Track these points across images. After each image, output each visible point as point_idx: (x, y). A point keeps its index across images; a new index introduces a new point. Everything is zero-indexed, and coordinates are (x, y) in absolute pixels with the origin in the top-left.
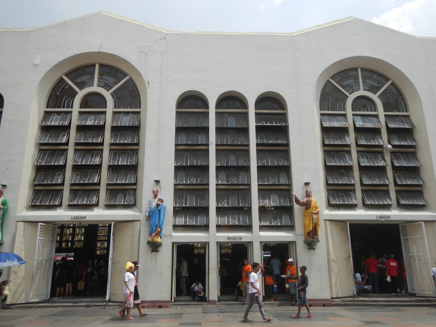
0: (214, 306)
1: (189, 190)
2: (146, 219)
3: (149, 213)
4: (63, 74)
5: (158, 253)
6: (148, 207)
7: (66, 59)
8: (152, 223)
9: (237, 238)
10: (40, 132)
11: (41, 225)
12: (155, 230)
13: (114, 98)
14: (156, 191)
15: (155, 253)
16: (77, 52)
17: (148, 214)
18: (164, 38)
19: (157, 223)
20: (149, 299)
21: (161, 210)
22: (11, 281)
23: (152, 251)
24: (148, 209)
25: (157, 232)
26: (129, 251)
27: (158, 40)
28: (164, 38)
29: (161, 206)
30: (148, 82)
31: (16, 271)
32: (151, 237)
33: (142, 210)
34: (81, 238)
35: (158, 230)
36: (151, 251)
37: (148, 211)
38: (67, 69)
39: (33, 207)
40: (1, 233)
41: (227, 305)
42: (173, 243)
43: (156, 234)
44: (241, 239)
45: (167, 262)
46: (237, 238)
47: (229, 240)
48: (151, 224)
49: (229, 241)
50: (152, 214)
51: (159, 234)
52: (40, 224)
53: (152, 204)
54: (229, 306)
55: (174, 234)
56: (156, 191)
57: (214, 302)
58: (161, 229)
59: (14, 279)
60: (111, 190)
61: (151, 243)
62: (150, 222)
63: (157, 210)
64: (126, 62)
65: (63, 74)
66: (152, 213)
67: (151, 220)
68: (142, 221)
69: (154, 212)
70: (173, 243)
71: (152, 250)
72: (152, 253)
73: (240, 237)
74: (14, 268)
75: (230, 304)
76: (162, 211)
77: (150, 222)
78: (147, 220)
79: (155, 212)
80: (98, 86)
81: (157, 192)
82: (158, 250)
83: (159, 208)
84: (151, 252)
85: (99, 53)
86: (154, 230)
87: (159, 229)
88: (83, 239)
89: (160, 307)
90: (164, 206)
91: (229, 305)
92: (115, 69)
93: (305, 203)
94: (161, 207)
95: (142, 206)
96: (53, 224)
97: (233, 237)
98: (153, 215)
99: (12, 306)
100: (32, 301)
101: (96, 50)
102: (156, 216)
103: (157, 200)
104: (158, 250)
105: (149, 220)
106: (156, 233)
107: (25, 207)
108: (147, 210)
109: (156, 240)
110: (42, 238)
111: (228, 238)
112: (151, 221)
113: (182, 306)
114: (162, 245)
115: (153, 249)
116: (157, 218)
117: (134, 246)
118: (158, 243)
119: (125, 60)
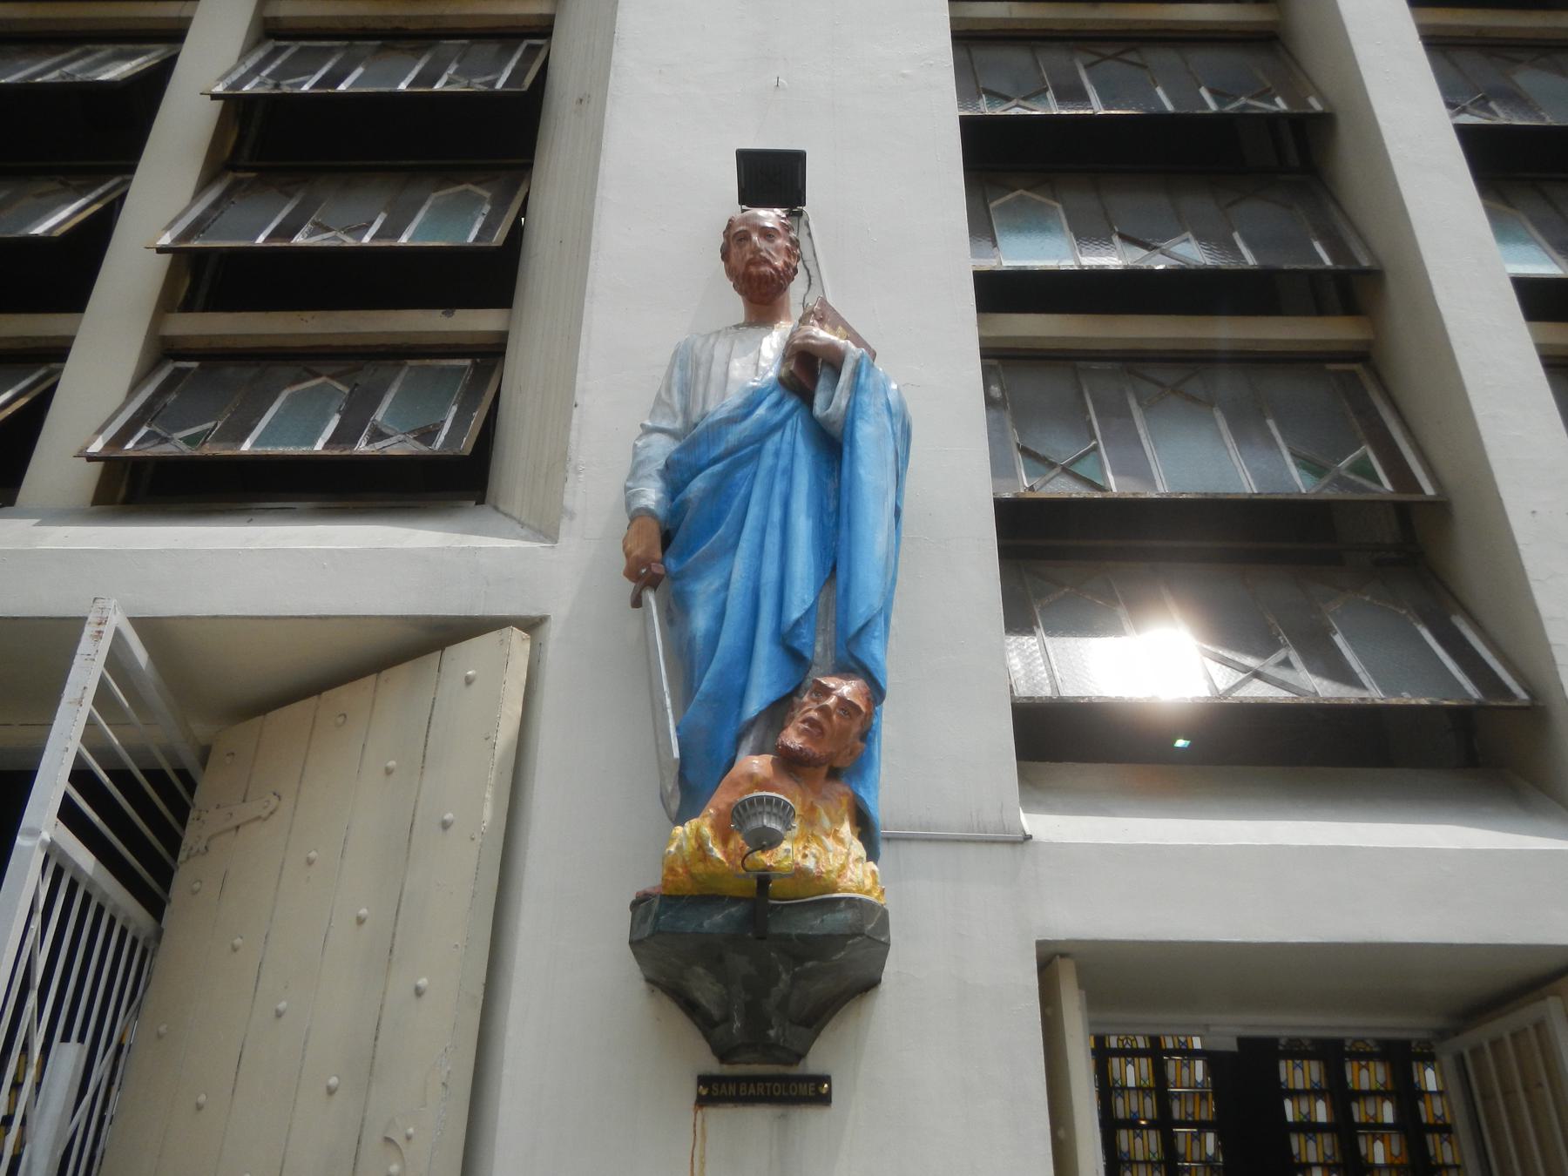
1: (1133, 361)
2: (632, 573)
3: (676, 476)
5: (810, 1119)
6: (648, 431)
8: (720, 616)
12: (779, 711)
15: (758, 1120)
17: (651, 495)
19: (801, 596)
24: (661, 448)
25: (815, 729)
26: (331, 1091)
29: (856, 373)
32: (722, 799)
33: (568, 501)
35: (827, 692)
36: (690, 1091)
37: (662, 461)
42: (1050, 960)
43: (791, 763)
48: (701, 621)
50: (720, 491)
51: (834, 774)
53: (717, 370)
55: (1043, 825)
58: (876, 692)
60: (216, 356)
61: (714, 921)
62: (677, 611)
63: (796, 426)
66: (725, 476)
67: (697, 574)
68: (553, 633)
69: (748, 453)
70: (1050, 960)
71: (713, 1066)
72: (720, 1117)
76: (870, 438)
77: (677, 611)
78: (643, 576)
79: (767, 460)
82: (814, 1063)
83: (830, 402)
84: (702, 1101)
86: (754, 706)
87: (847, 688)
94: (855, 388)
95: (563, 457)
98: (736, 502)
102: (776, 513)
103: (772, 344)
104: (814, 1063)
105: (678, 577)
106: (793, 738)
108: (635, 455)
109: (789, 854)
112: (703, 591)
114: (870, 984)
115: (723, 1055)
116: (803, 527)
117: (419, 992)
118: (844, 917)
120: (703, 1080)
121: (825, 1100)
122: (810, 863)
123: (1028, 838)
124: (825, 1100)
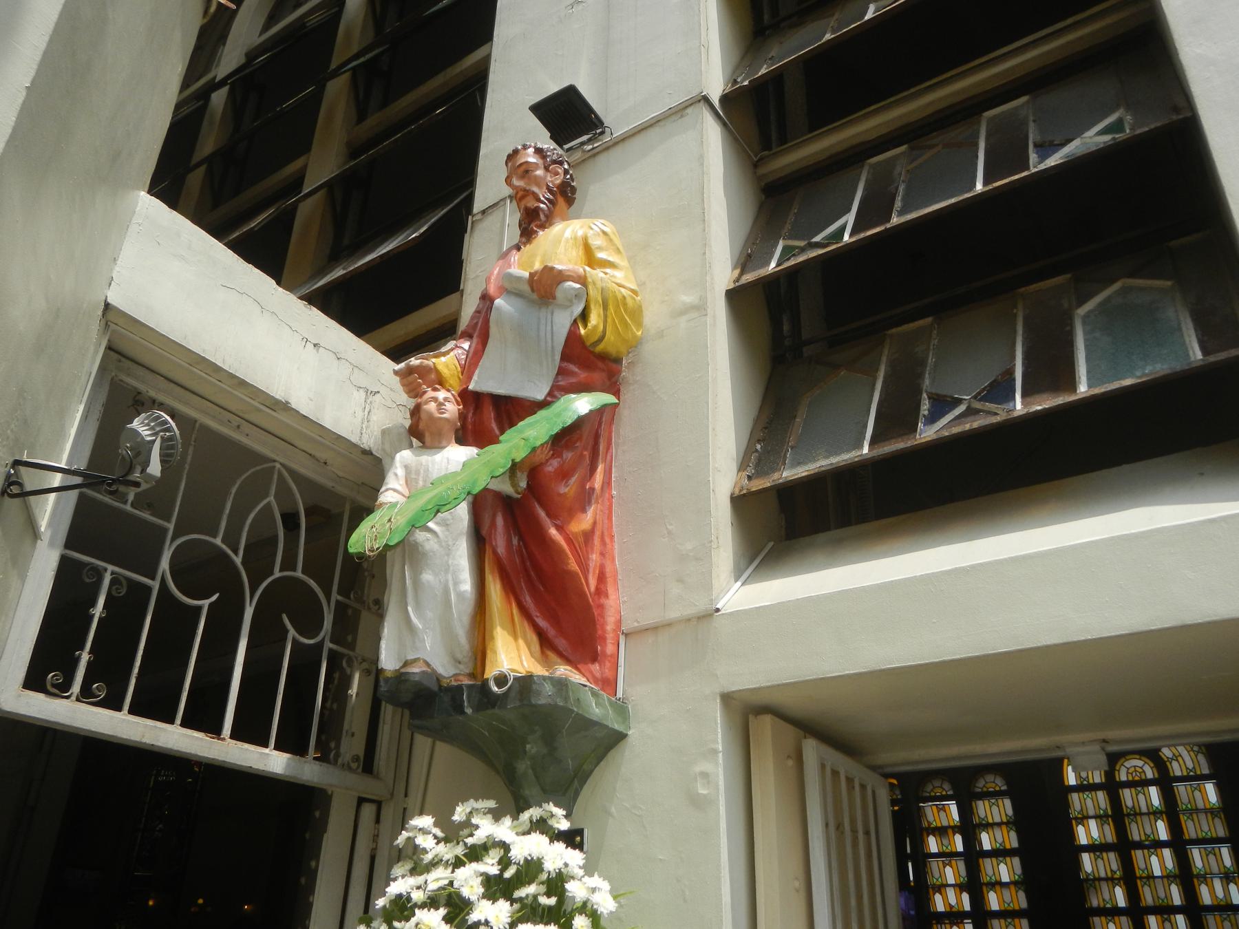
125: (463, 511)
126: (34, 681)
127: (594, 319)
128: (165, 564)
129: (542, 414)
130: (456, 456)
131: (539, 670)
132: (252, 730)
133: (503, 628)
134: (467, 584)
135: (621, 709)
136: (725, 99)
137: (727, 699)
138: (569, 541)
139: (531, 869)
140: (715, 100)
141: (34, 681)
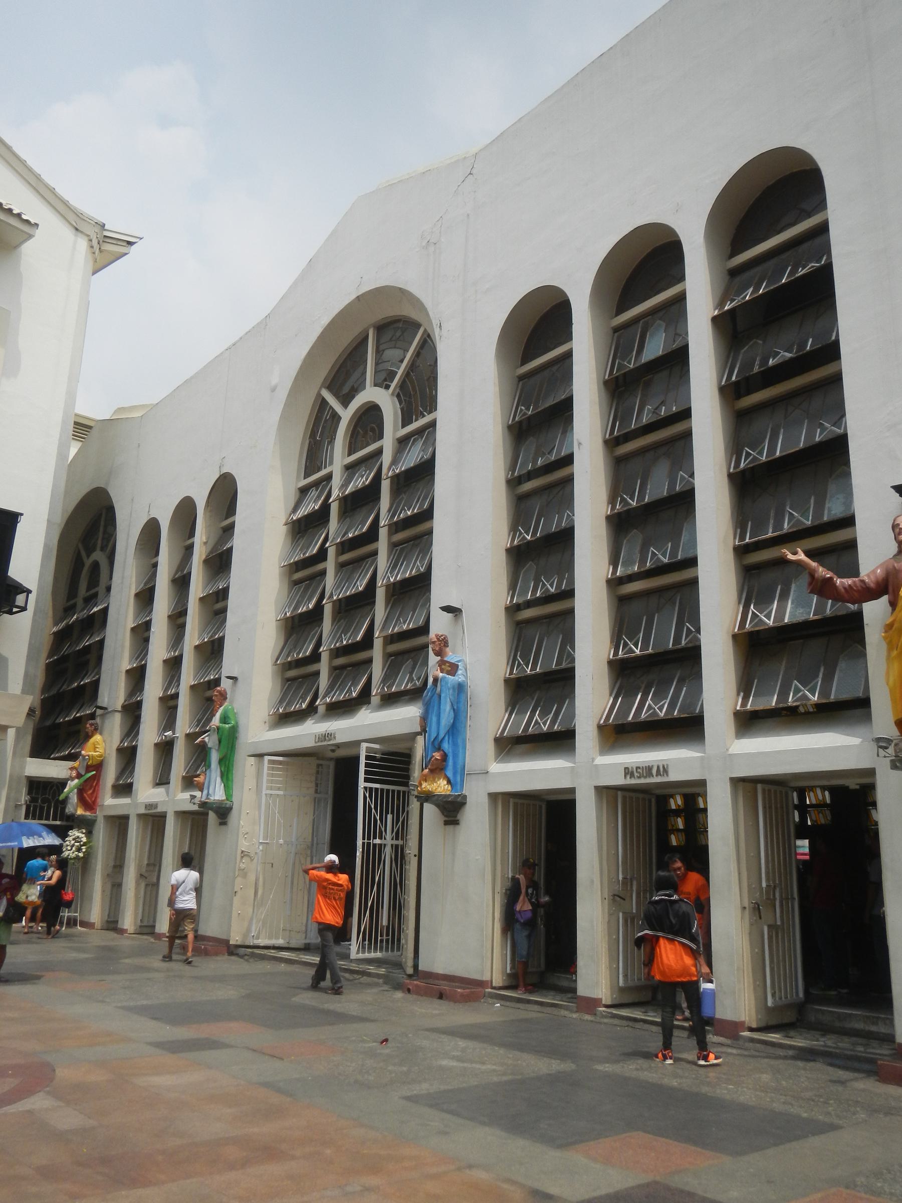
0: (588, 1017)
4: (320, 388)
5: (457, 826)
7: (312, 348)
9: (654, 771)
10: (289, 541)
11: (270, 762)
13: (400, 402)
14: (436, 640)
15: (451, 827)
16: (326, 320)
18: (470, 174)
20: (441, 972)
21: (443, 695)
22: (236, 892)
23: (446, 823)
27: (459, 186)
28: (470, 174)
30: (440, 323)
31: (245, 871)
34: (824, 796)
38: (323, 371)
39: (285, 718)
40: (223, 784)
41: (624, 1022)
43: (431, 771)
44: (667, 775)
45: (477, 858)
46: (654, 771)
47: (628, 777)
49: (630, 781)
52: (267, 758)
54: (630, 1029)
55: (496, 768)
56: (436, 640)
57: (590, 1004)
59: (241, 888)
64: (402, 292)
65: (319, 386)
72: (446, 826)
73: (663, 766)
74: (242, 864)
75: (635, 1020)
80: (375, 385)
81: (437, 643)
85: (359, 300)
88: (828, 801)
89: (441, 996)
90: (450, 681)
91: (631, 1024)
92: (402, 322)
93: (872, 585)
96: (318, 759)
97: (639, 768)
99: (242, 951)
100: (262, 942)
101: (353, 297)
107: (265, 722)
110: (281, 793)
111: (628, 772)
113: (508, 1004)
119: (400, 289)
120: (445, 821)
121: (458, 824)
122: (430, 789)
123: (488, 772)
124: (458, 824)
125: (76, 790)
126: (25, 819)
127: (91, 762)
128: (40, 801)
129: (84, 777)
130: (76, 781)
131: (84, 813)
132: (55, 819)
133: (81, 807)
134: (76, 801)
135: (96, 817)
136: (124, 707)
137: (105, 816)
138: (87, 795)
139: (78, 837)
140: (119, 708)
141: (25, 819)
